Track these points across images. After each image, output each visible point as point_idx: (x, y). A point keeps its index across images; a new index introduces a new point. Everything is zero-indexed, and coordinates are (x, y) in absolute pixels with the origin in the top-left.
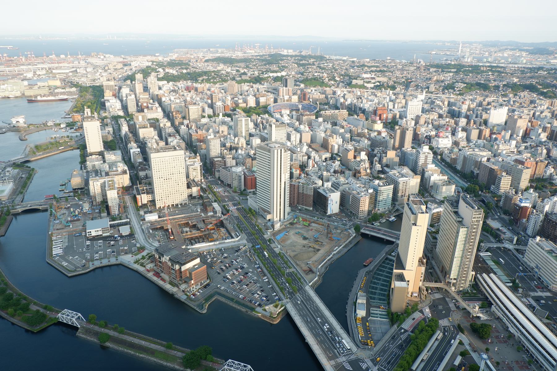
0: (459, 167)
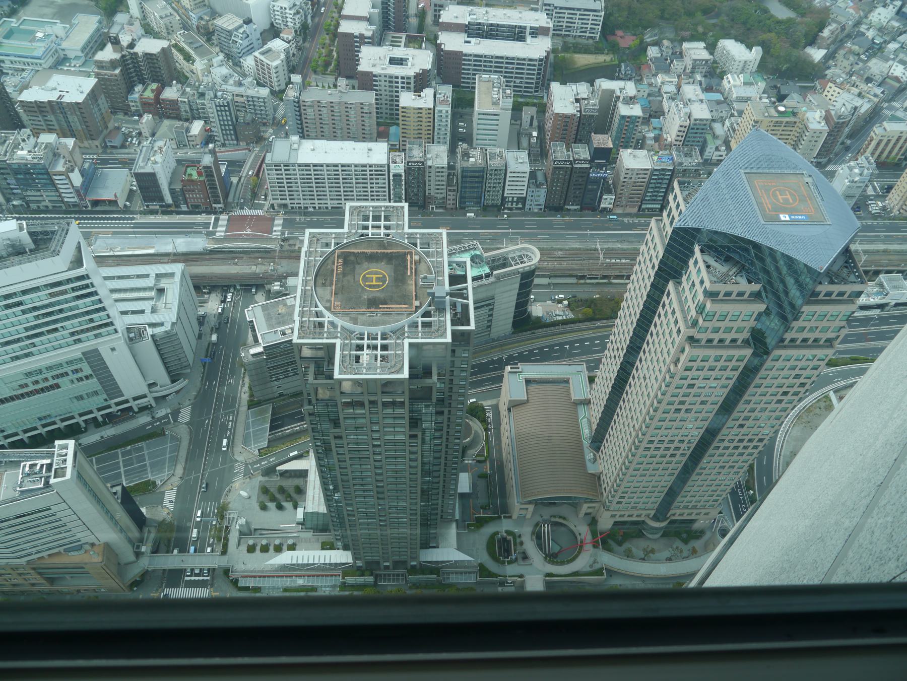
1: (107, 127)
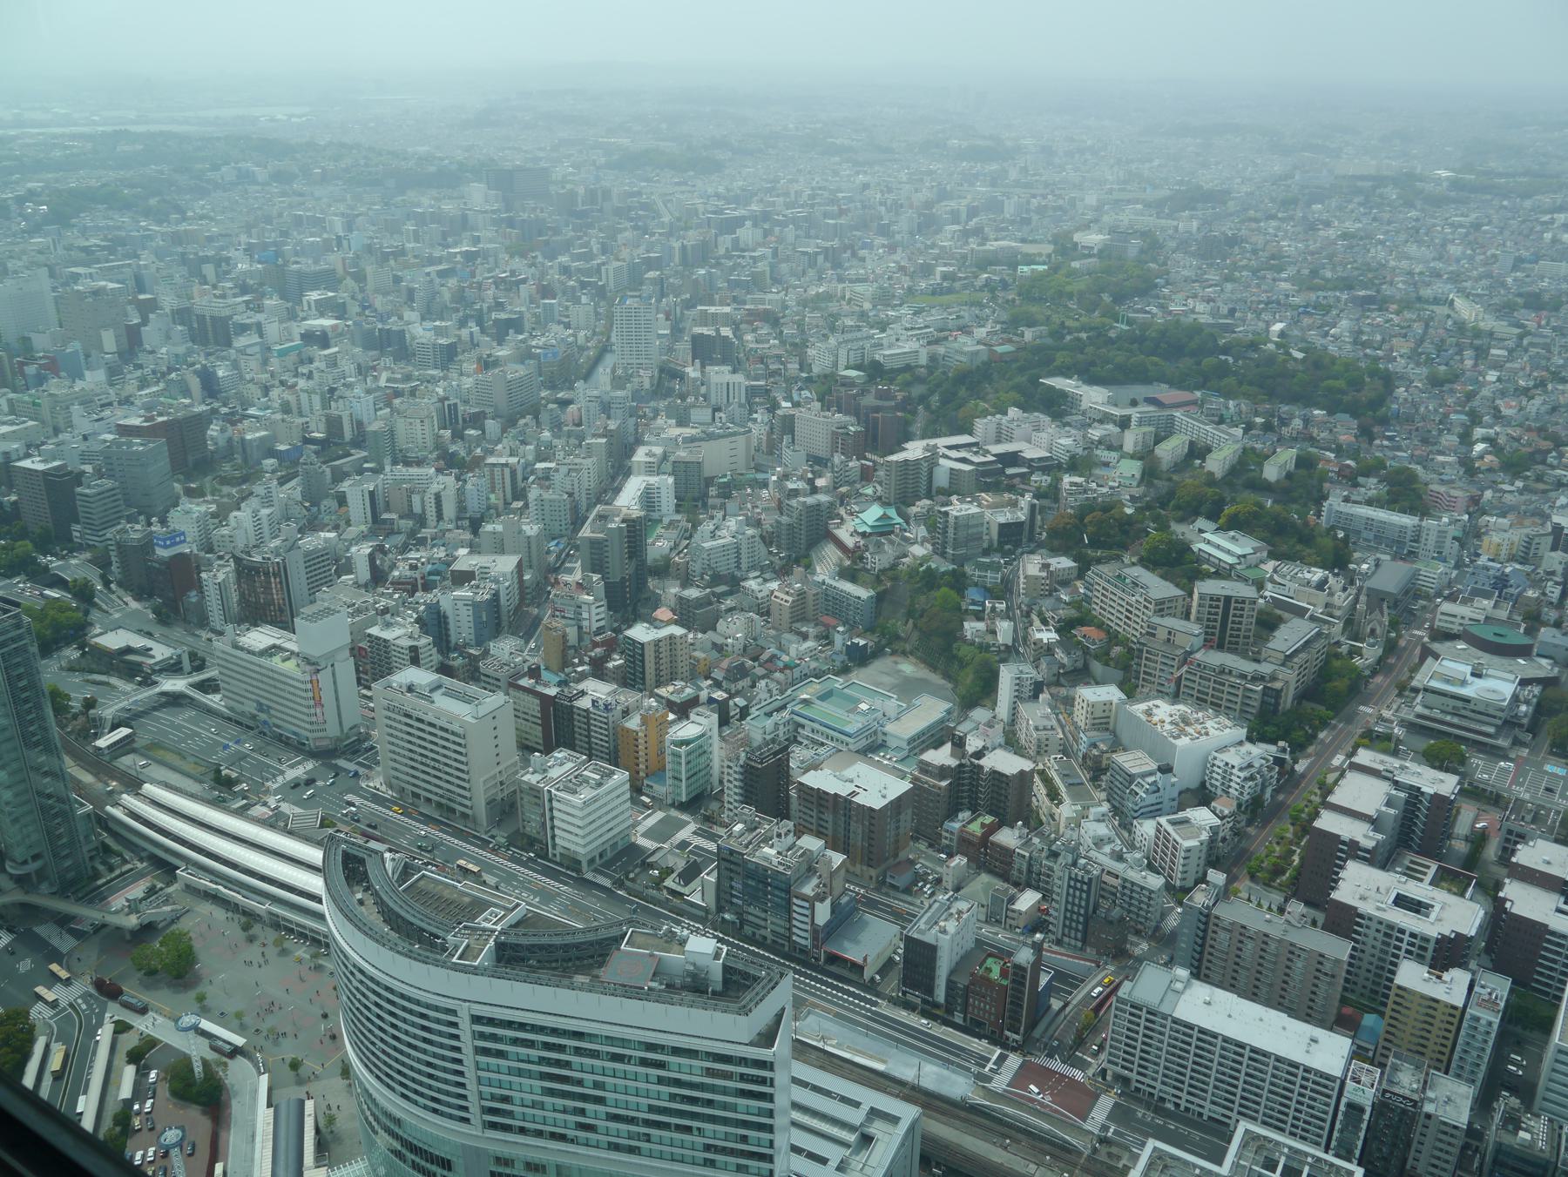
1: (896, 855)
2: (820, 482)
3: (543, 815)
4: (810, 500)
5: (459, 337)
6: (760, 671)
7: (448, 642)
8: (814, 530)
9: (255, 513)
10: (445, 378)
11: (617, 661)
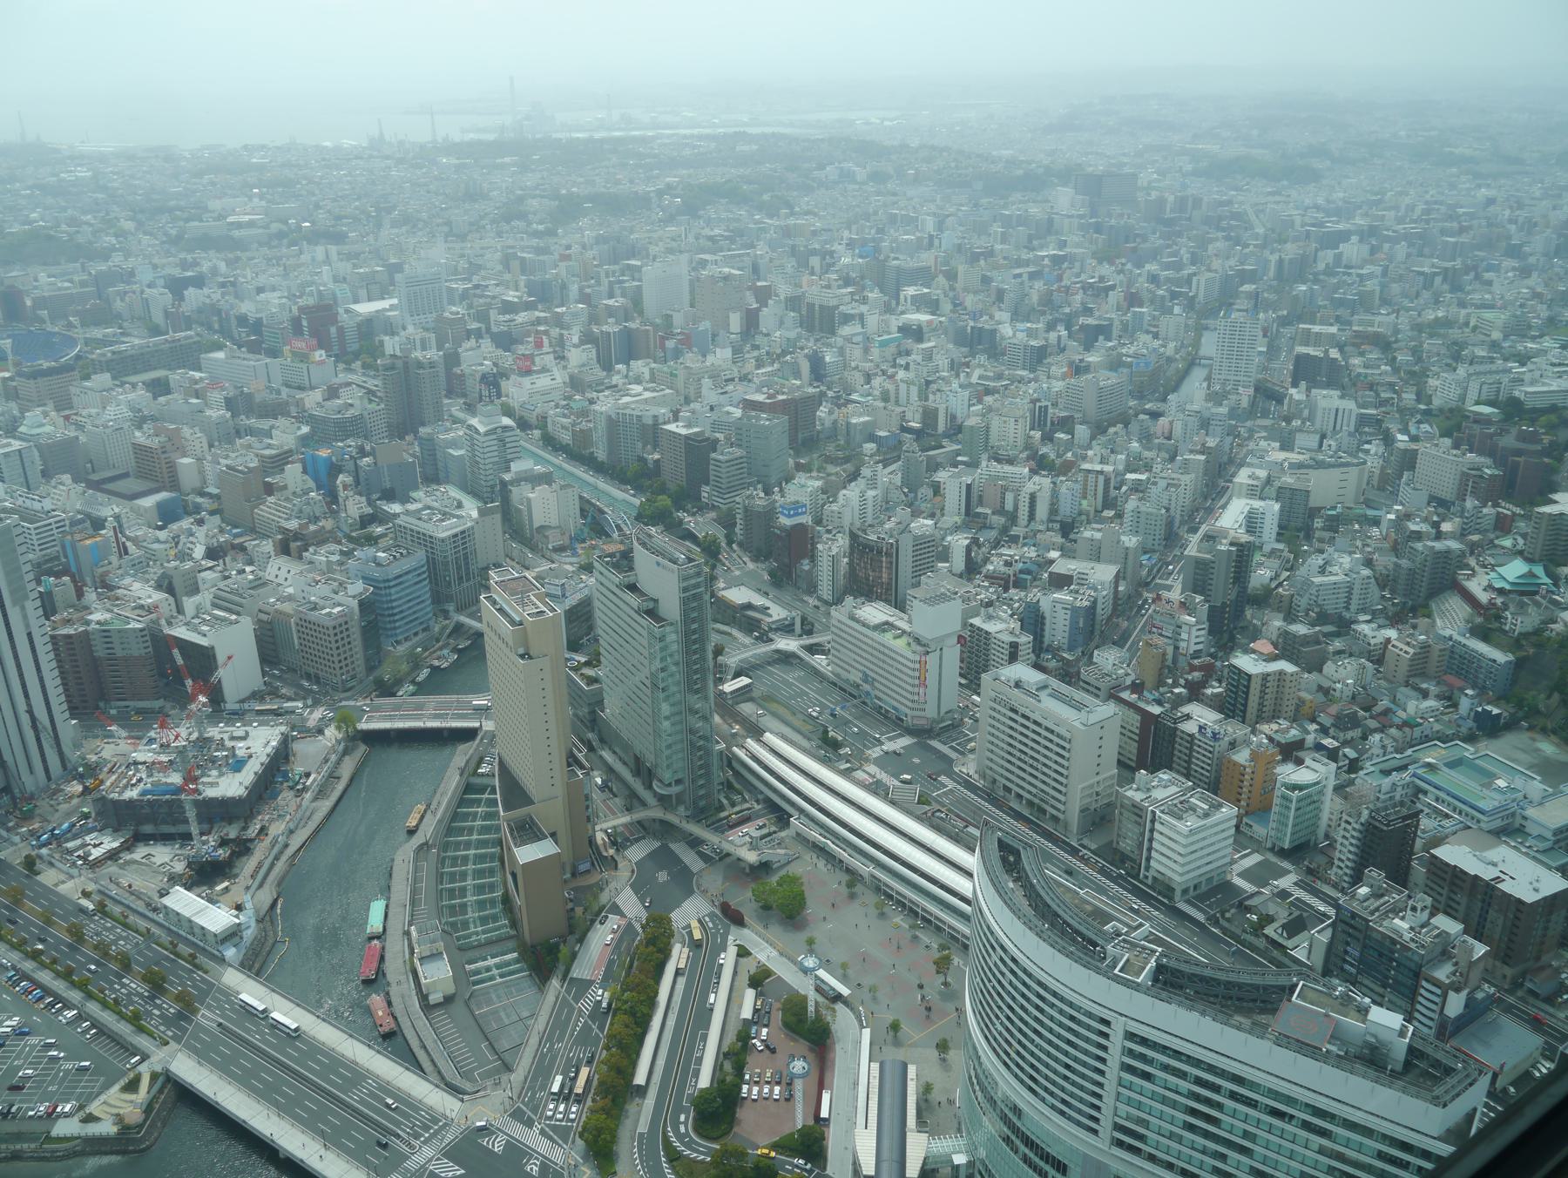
0: (601, 454)
1: (1538, 958)
2: (1446, 527)
3: (1143, 834)
4: (1438, 545)
5: (1046, 340)
6: (1373, 724)
7: (1042, 642)
8: (1443, 578)
9: (863, 494)
10: (1036, 380)
11: (1214, 689)
